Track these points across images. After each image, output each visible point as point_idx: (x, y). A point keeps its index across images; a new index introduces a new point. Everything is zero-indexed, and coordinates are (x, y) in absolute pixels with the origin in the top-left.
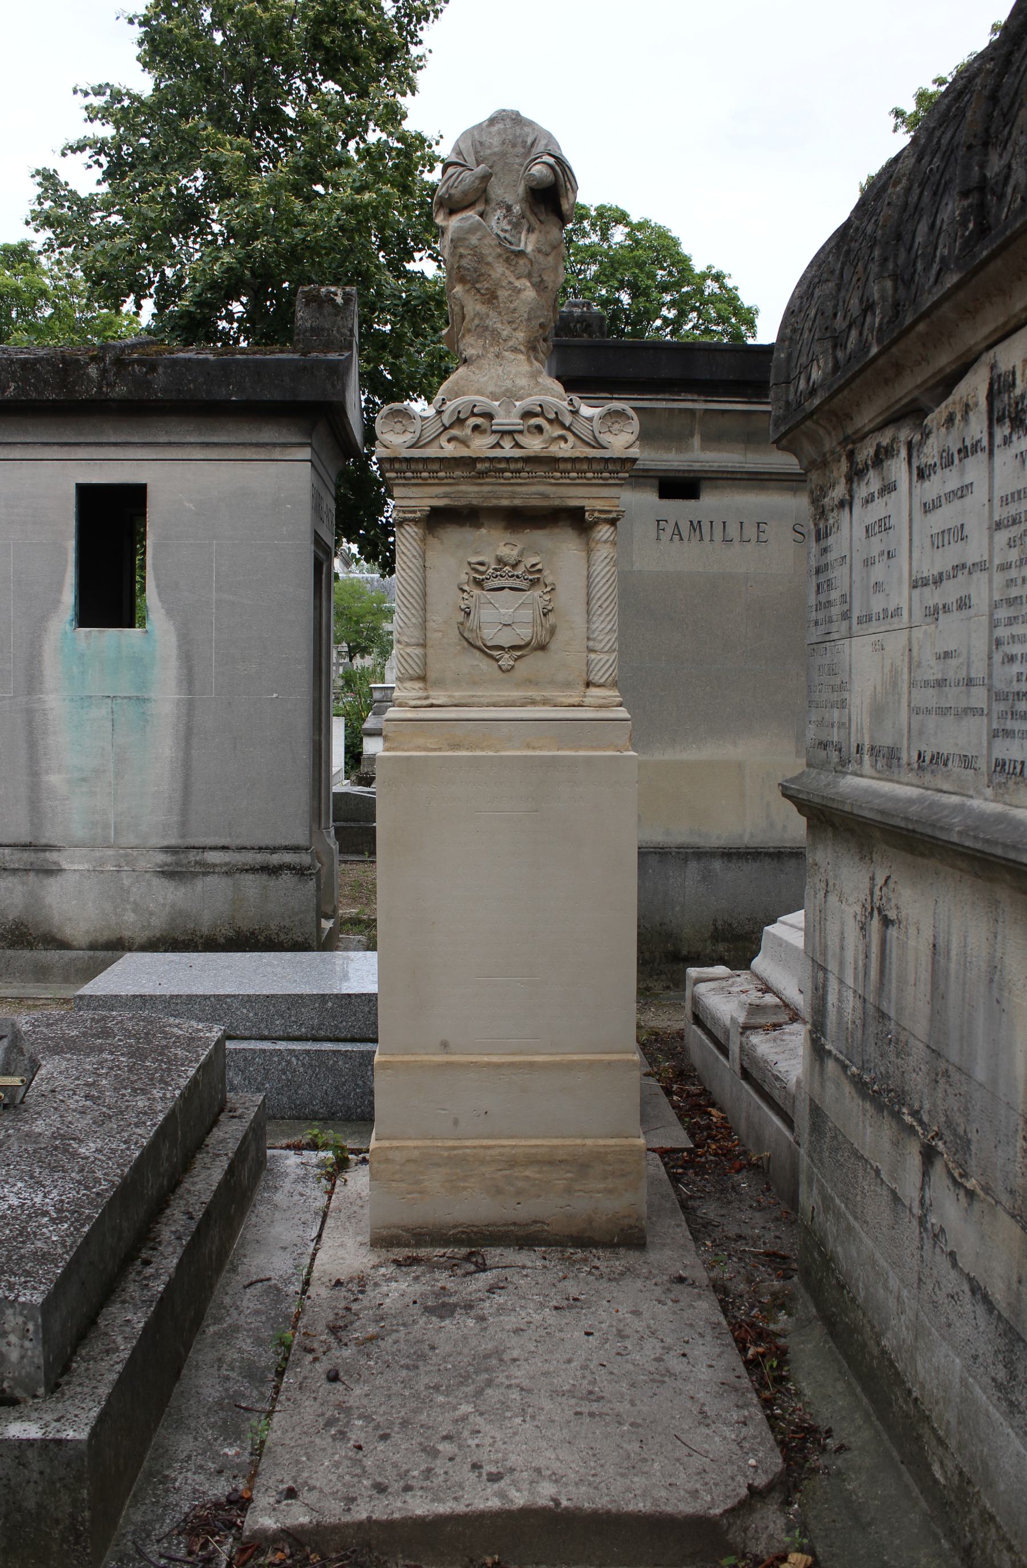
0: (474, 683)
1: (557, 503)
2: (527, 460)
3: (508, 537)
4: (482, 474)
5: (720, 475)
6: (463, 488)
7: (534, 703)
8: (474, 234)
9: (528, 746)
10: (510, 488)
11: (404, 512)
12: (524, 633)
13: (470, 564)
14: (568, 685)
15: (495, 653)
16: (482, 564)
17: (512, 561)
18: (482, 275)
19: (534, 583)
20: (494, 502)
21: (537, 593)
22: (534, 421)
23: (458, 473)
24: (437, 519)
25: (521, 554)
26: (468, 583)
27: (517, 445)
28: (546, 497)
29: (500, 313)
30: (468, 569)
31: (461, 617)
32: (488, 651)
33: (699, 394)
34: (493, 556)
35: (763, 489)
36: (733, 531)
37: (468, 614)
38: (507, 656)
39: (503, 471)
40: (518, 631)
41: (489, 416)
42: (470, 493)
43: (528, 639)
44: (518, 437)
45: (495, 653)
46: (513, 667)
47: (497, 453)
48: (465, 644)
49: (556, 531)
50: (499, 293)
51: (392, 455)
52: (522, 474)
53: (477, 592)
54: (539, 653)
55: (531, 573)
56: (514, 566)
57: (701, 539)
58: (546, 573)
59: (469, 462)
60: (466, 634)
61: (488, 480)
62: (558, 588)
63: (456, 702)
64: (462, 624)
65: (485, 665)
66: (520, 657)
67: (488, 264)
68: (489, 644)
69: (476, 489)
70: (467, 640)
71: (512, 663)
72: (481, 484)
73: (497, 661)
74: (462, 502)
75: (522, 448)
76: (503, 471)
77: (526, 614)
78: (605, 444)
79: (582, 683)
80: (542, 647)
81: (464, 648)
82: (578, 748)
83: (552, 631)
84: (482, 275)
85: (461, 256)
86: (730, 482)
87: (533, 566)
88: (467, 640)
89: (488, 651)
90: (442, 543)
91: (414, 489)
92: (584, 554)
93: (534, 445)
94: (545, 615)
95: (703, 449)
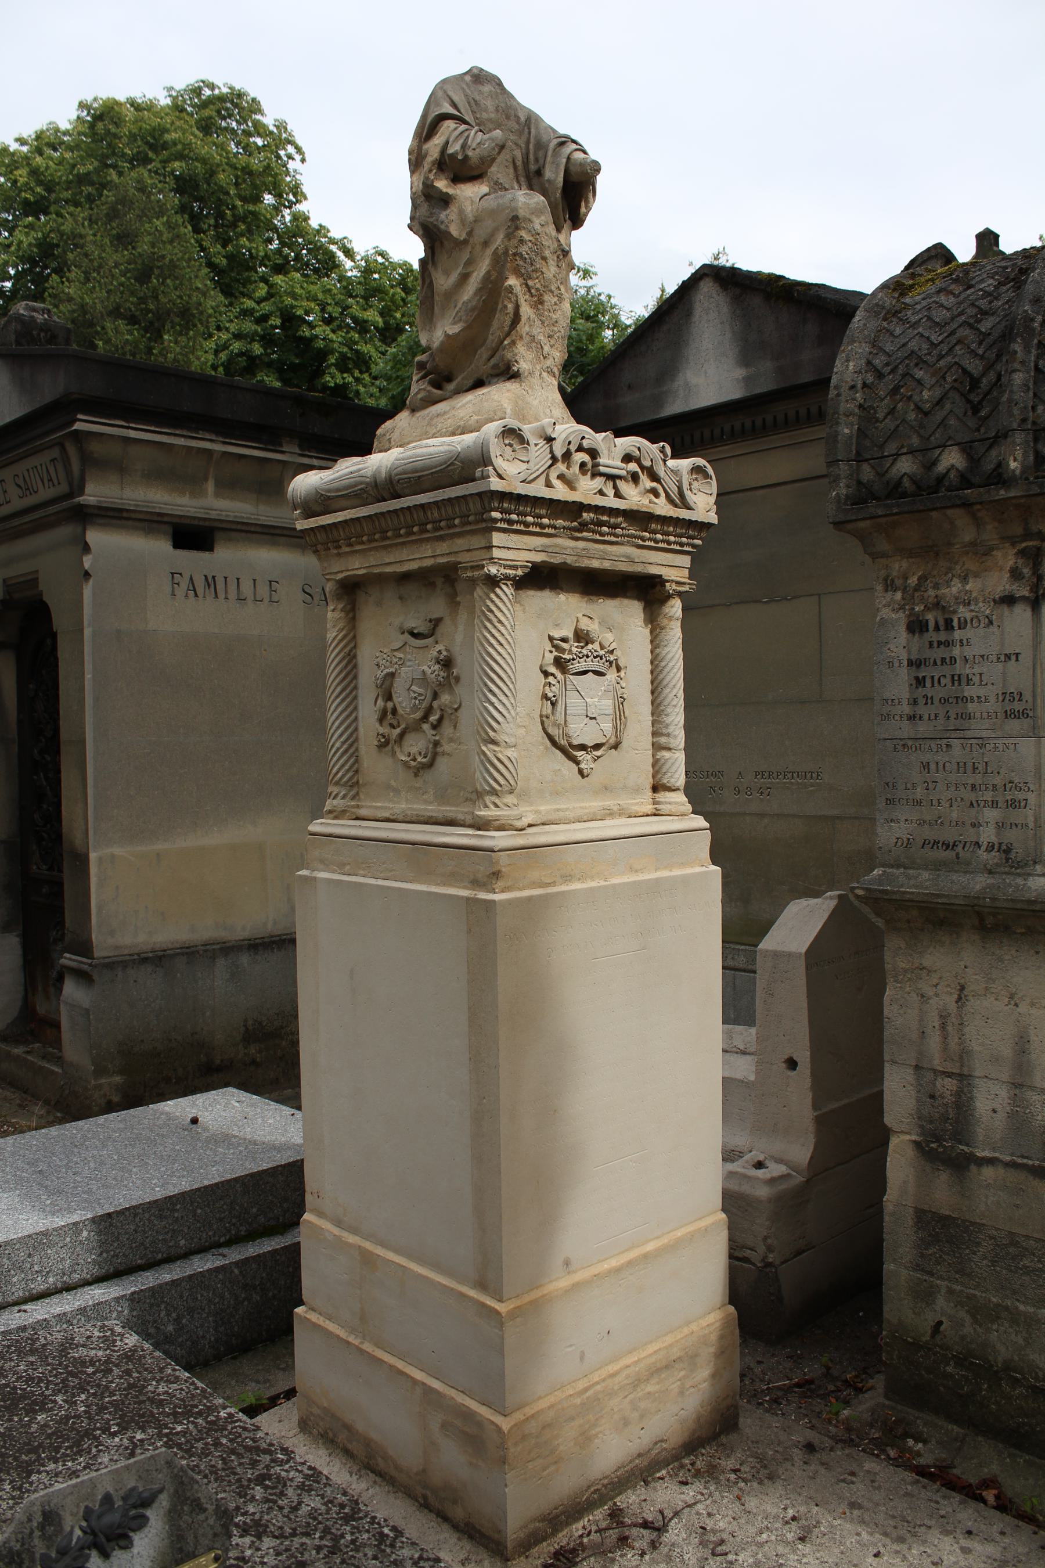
1: (639, 569)
4: (583, 526)
5: (234, 527)
6: (558, 541)
7: (610, 814)
8: (538, 217)
13: (551, 639)
14: (637, 790)
18: (536, 270)
20: (586, 563)
22: (633, 466)
24: (541, 577)
27: (618, 495)
29: (543, 323)
30: (548, 646)
33: (217, 434)
35: (274, 544)
36: (247, 588)
39: (602, 524)
41: (593, 453)
44: (621, 484)
47: (600, 501)
50: (546, 297)
51: (508, 490)
52: (619, 531)
57: (216, 596)
59: (573, 510)
60: (550, 731)
61: (585, 534)
63: (544, 819)
67: (544, 259)
68: (575, 742)
69: (572, 543)
72: (577, 539)
74: (557, 560)
76: (602, 524)
78: (692, 505)
79: (649, 787)
80: (616, 746)
81: (546, 748)
82: (669, 867)
84: (536, 270)
85: (522, 241)
86: (243, 535)
91: (514, 537)
93: (634, 497)
95: (217, 495)
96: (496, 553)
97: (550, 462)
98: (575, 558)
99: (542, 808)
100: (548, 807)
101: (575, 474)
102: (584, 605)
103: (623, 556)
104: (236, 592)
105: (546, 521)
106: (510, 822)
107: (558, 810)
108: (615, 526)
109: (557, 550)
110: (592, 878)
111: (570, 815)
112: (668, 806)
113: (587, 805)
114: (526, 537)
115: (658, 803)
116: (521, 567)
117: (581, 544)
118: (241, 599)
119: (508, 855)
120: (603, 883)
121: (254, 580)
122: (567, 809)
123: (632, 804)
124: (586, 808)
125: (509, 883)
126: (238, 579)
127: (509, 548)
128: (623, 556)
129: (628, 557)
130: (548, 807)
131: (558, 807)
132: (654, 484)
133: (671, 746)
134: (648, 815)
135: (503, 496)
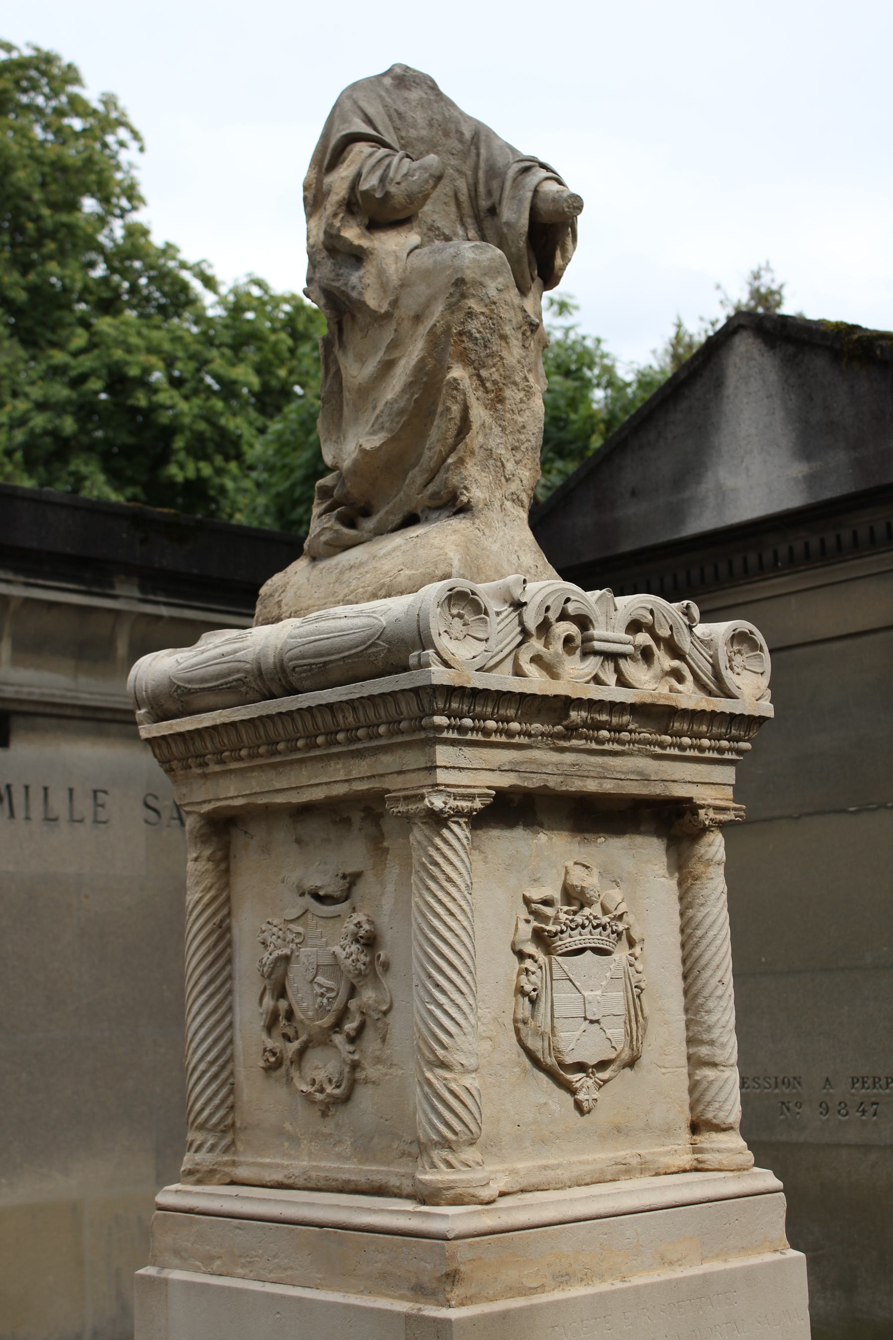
0: (543, 1141)
1: (657, 790)
2: (635, 709)
4: (572, 731)
5: (41, 709)
7: (626, 1171)
8: (493, 278)
9: (666, 1262)
10: (599, 760)
11: (456, 797)
13: (527, 901)
14: (667, 1131)
18: (492, 355)
22: (643, 638)
23: (536, 727)
27: (622, 682)
28: (646, 779)
29: (504, 429)
30: (524, 913)
33: (16, 571)
35: (101, 734)
39: (599, 726)
41: (583, 622)
42: (549, 766)
44: (626, 666)
48: (527, 1062)
50: (508, 393)
51: (457, 683)
52: (625, 735)
57: (12, 815)
58: (629, 918)
59: (556, 707)
60: (530, 1043)
61: (574, 742)
63: (524, 1183)
67: (504, 337)
68: (569, 1060)
69: (555, 757)
72: (562, 750)
74: (533, 782)
76: (599, 726)
78: (735, 691)
80: (631, 1064)
81: (525, 1071)
84: (492, 355)
85: (470, 314)
86: (54, 721)
91: (468, 751)
92: (673, 883)
93: (648, 684)
95: (15, 662)
96: (442, 777)
97: (520, 638)
98: (560, 779)
99: (520, 1165)
100: (529, 1164)
101: (557, 654)
103: (633, 772)
104: (42, 808)
105: (515, 726)
106: (471, 1191)
107: (545, 1167)
108: (619, 729)
109: (533, 768)
110: (602, 1278)
111: (564, 1175)
112: (718, 1156)
113: (589, 1157)
115: (701, 1151)
116: (480, 796)
117: (569, 758)
118: (50, 820)
120: (619, 1285)
121: (71, 790)
122: (559, 1166)
124: (587, 1163)
125: (472, 1291)
126: (46, 789)
127: (460, 769)
128: (633, 772)
129: (639, 773)
130: (529, 1164)
131: (544, 1162)
132: (676, 663)
133: (717, 1060)
134: (685, 1171)
135: (450, 692)
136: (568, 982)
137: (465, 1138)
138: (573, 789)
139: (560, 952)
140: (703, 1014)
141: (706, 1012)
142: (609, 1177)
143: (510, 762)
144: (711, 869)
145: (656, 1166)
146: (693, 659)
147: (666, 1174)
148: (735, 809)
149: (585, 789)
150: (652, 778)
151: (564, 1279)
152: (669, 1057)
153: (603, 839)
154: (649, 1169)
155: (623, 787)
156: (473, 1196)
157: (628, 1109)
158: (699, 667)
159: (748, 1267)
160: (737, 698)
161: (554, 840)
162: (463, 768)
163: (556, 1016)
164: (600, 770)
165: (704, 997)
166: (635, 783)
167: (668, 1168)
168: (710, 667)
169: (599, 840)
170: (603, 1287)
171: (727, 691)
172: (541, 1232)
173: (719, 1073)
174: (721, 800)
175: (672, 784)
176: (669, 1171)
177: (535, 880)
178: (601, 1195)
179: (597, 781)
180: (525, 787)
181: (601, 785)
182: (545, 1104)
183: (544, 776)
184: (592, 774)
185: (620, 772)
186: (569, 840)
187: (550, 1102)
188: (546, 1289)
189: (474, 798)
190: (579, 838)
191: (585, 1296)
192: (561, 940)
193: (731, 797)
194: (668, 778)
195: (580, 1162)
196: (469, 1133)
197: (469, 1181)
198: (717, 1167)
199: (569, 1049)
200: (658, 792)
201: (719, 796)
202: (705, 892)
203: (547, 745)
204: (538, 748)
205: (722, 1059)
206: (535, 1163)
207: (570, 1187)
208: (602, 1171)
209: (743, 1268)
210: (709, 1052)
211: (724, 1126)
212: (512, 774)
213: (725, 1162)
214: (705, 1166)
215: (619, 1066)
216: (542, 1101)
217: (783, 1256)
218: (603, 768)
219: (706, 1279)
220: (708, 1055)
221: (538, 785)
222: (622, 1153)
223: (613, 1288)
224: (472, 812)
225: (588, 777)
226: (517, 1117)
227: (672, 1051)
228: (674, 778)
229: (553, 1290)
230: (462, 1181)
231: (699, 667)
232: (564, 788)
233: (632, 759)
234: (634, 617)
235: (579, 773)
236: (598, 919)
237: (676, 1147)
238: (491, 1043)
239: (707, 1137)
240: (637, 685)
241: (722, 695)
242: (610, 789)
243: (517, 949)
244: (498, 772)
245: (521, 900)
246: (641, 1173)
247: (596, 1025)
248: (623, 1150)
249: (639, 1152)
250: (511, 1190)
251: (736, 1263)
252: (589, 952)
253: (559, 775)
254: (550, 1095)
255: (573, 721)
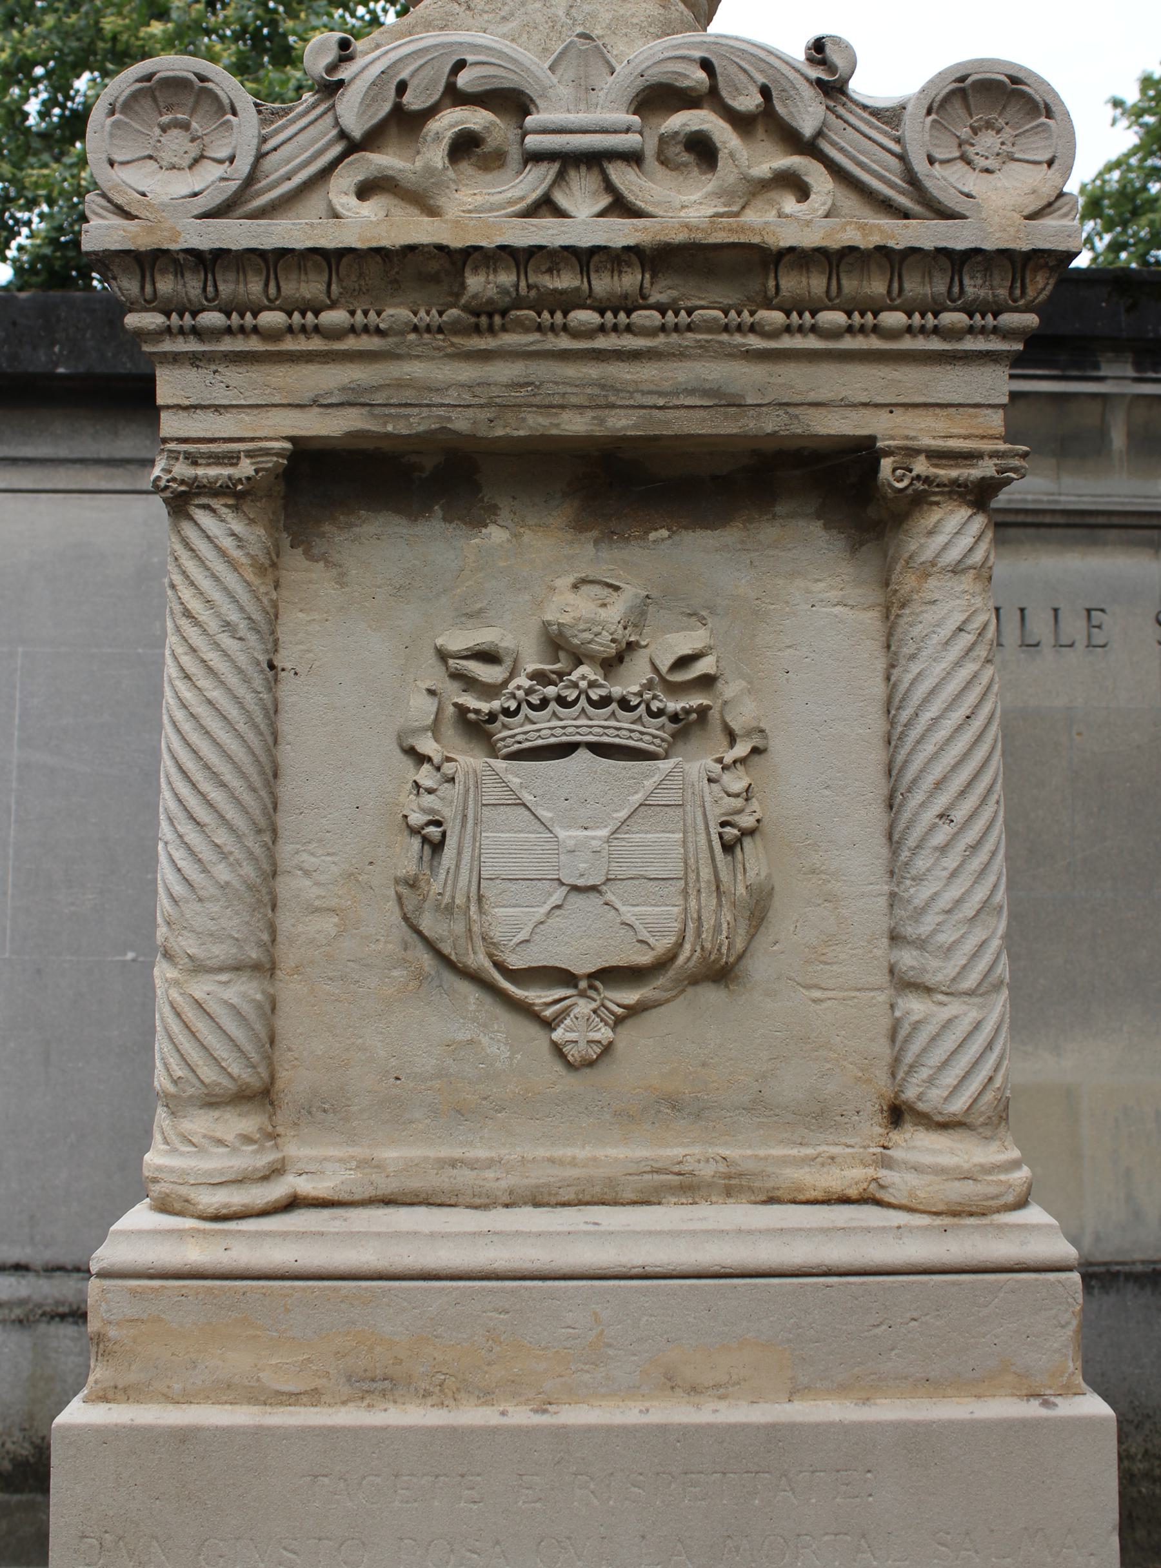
1: (771, 423)
2: (659, 259)
3: (588, 555)
4: (488, 316)
6: (415, 370)
7: (687, 1188)
9: (672, 1383)
10: (593, 371)
11: (193, 460)
12: (647, 920)
13: (443, 656)
14: (819, 1116)
15: (537, 996)
16: (488, 656)
17: (603, 645)
19: (686, 727)
20: (534, 423)
21: (696, 763)
25: (637, 617)
26: (435, 728)
27: (621, 206)
28: (733, 403)
30: (435, 676)
31: (407, 856)
32: (513, 987)
34: (534, 625)
35: (1094, 543)
36: (1040, 626)
37: (437, 847)
38: (583, 1007)
39: (567, 302)
40: (628, 913)
41: (512, 102)
42: (445, 388)
43: (663, 944)
44: (623, 176)
45: (537, 996)
46: (608, 1049)
47: (546, 232)
48: (426, 960)
49: (768, 531)
51: (145, 243)
52: (642, 317)
53: (469, 761)
54: (711, 995)
55: (674, 689)
56: (611, 664)
58: (729, 689)
59: (436, 269)
60: (427, 924)
62: (776, 744)
63: (387, 1185)
64: (412, 884)
65: (500, 1040)
66: (634, 1011)
68: (516, 962)
69: (467, 372)
70: (431, 945)
71: (604, 1034)
72: (485, 356)
73: (549, 1025)
74: (416, 423)
75: (637, 213)
76: (567, 302)
77: (661, 846)
79: (872, 1108)
80: (720, 973)
81: (420, 977)
83: (758, 910)
87: (684, 662)
88: (431, 945)
89: (513, 987)
90: (341, 581)
91: (234, 375)
92: (871, 619)
93: (682, 206)
94: (728, 848)
96: (170, 425)
97: (337, 149)
98: (488, 414)
99: (390, 1154)
100: (416, 1152)
101: (429, 170)
102: (590, 550)
103: (691, 392)
104: (1018, 632)
105: (335, 317)
106: (183, 1190)
107: (453, 1163)
108: (627, 304)
109: (408, 395)
110: (486, 1396)
111: (496, 1181)
112: (912, 1179)
113: (600, 1153)
114: (266, 368)
115: (886, 1163)
116: (250, 454)
117: (504, 372)
118: (1030, 646)
119: (134, 1292)
120: (521, 1416)
121: (1056, 610)
122: (490, 1163)
123: (786, 1161)
124: (573, 1162)
125: (132, 1377)
126: (1022, 610)
127: (218, 408)
128: (691, 392)
129: (706, 393)
130: (416, 1152)
131: (457, 1153)
132: (794, 161)
133: (929, 979)
134: (845, 1200)
135: (148, 261)
136: (522, 810)
137: (191, 1091)
138: (522, 433)
139: (505, 751)
140: (908, 882)
141: (913, 879)
142: (630, 1195)
143: (343, 389)
144: (932, 582)
145: (770, 1184)
146: (841, 150)
147: (794, 1202)
148: (994, 454)
149: (554, 432)
150: (749, 401)
151: (379, 1385)
152: (835, 967)
153: (664, 533)
154: (751, 1189)
155: (667, 423)
156: (187, 1201)
157: (704, 1065)
158: (860, 164)
159: (918, 1424)
160: (964, 217)
161: (526, 539)
162: (225, 407)
163: (484, 874)
164: (597, 391)
165: (910, 849)
166: (702, 413)
167: (800, 1190)
168: (894, 162)
169: (652, 536)
170: (472, 1415)
171: (937, 206)
172: (304, 1289)
173: (935, 1008)
174: (966, 437)
175: (812, 411)
176: (801, 1197)
177: (470, 616)
178: (518, 1233)
179: (590, 414)
180: (388, 435)
181: (602, 421)
182: (471, 1042)
183: (441, 412)
184: (574, 400)
185: (651, 393)
186: (569, 537)
187: (485, 1040)
188: (324, 1398)
189: (239, 458)
190: (595, 533)
191: (410, 1429)
192: (505, 727)
193: (1001, 430)
194: (797, 399)
195: (552, 1161)
196: (198, 1084)
197: (184, 1172)
198: (904, 1202)
199: (516, 940)
200: (769, 428)
201: (955, 431)
202: (916, 631)
203: (439, 349)
204: (418, 357)
205: (939, 977)
206: (432, 1153)
207: (507, 1206)
208: (611, 1182)
209: (897, 1425)
210: (915, 963)
211: (939, 1118)
212: (353, 412)
213: (921, 1194)
214: (886, 1196)
215: (677, 981)
216: (463, 1035)
217: (1044, 1412)
218: (603, 387)
219: (775, 1435)
220: (913, 968)
221: (421, 428)
222: (678, 1152)
223: (504, 1421)
224: (235, 485)
225: (563, 407)
226: (394, 1062)
227: (843, 956)
228: (812, 397)
229: (344, 1403)
230: (172, 1170)
231: (860, 164)
232: (499, 432)
233: (688, 364)
234: (654, 80)
235: (536, 400)
236: (601, 686)
237: (834, 1150)
238: (336, 920)
239: (908, 1136)
240: (650, 209)
241: (932, 215)
242: (624, 428)
243: (407, 748)
244: (317, 410)
245: (432, 652)
246: (729, 1195)
247: (593, 896)
248: (682, 1145)
249: (726, 1152)
250: (345, 1197)
251: (888, 1410)
252: (583, 754)
253: (482, 406)
254: (485, 1026)
255: (475, 296)
